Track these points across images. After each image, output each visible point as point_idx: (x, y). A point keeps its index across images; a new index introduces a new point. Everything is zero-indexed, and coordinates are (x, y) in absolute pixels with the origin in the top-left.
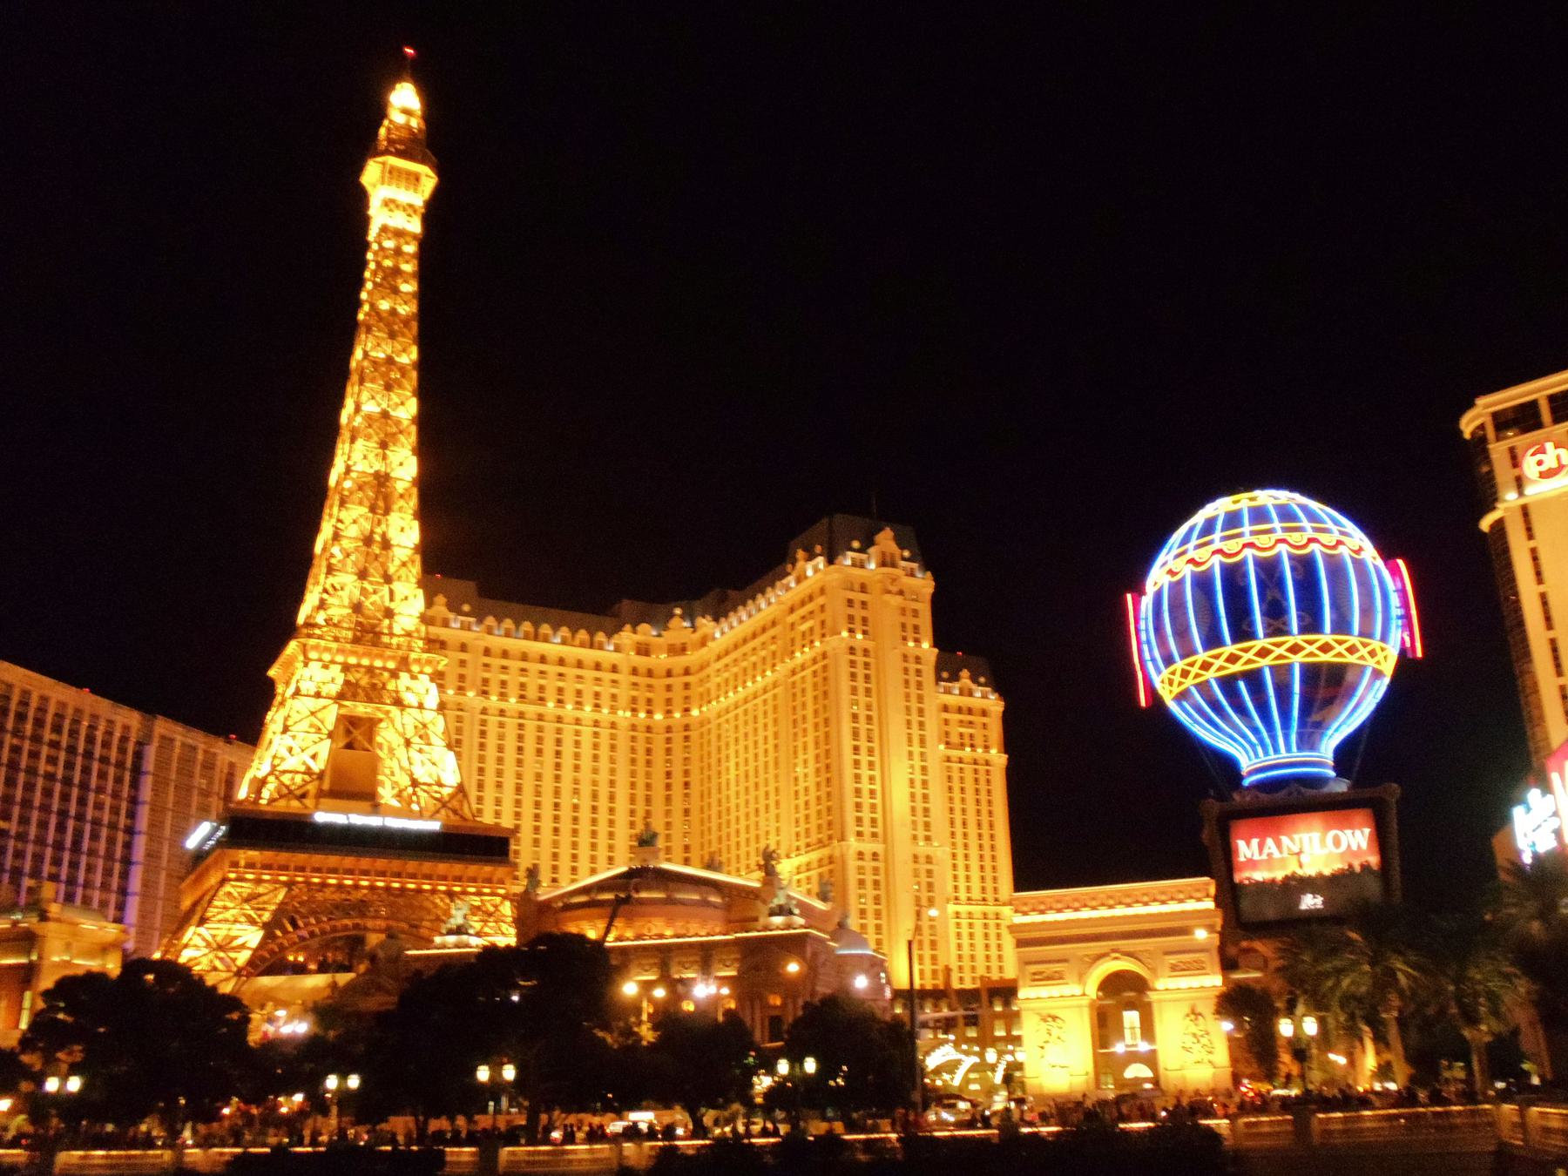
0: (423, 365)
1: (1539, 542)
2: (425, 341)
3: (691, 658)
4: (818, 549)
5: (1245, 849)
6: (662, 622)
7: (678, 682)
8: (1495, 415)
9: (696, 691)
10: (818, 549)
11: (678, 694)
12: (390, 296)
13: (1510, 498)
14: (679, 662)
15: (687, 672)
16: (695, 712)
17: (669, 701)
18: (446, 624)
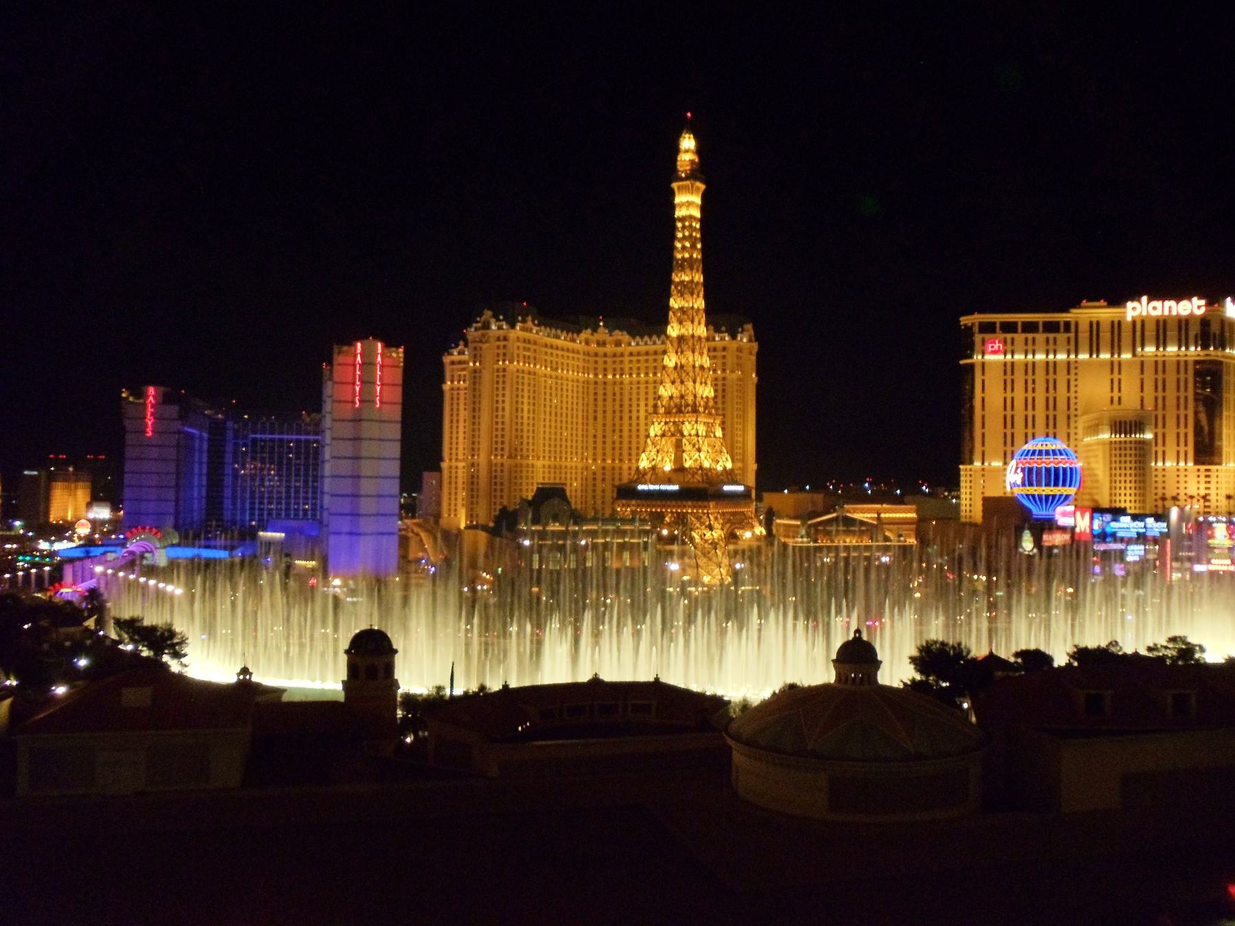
0: (706, 284)
1: (987, 378)
2: (705, 273)
3: (610, 349)
4: (723, 329)
5: (1045, 537)
6: (595, 330)
7: (600, 360)
8: (980, 324)
9: (610, 366)
10: (723, 329)
11: (601, 366)
12: (687, 246)
13: (977, 358)
14: (601, 350)
15: (605, 355)
16: (610, 377)
17: (596, 369)
18: (531, 331)
